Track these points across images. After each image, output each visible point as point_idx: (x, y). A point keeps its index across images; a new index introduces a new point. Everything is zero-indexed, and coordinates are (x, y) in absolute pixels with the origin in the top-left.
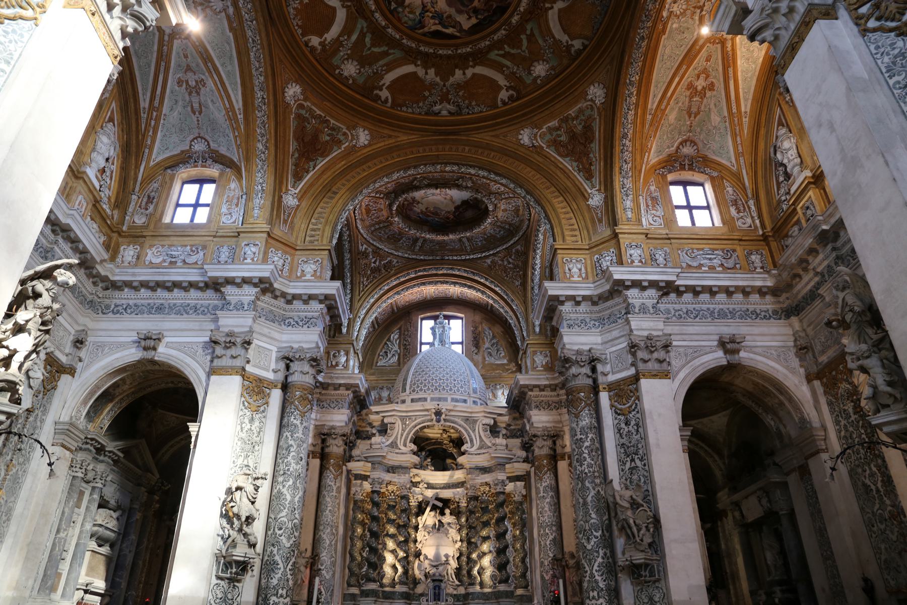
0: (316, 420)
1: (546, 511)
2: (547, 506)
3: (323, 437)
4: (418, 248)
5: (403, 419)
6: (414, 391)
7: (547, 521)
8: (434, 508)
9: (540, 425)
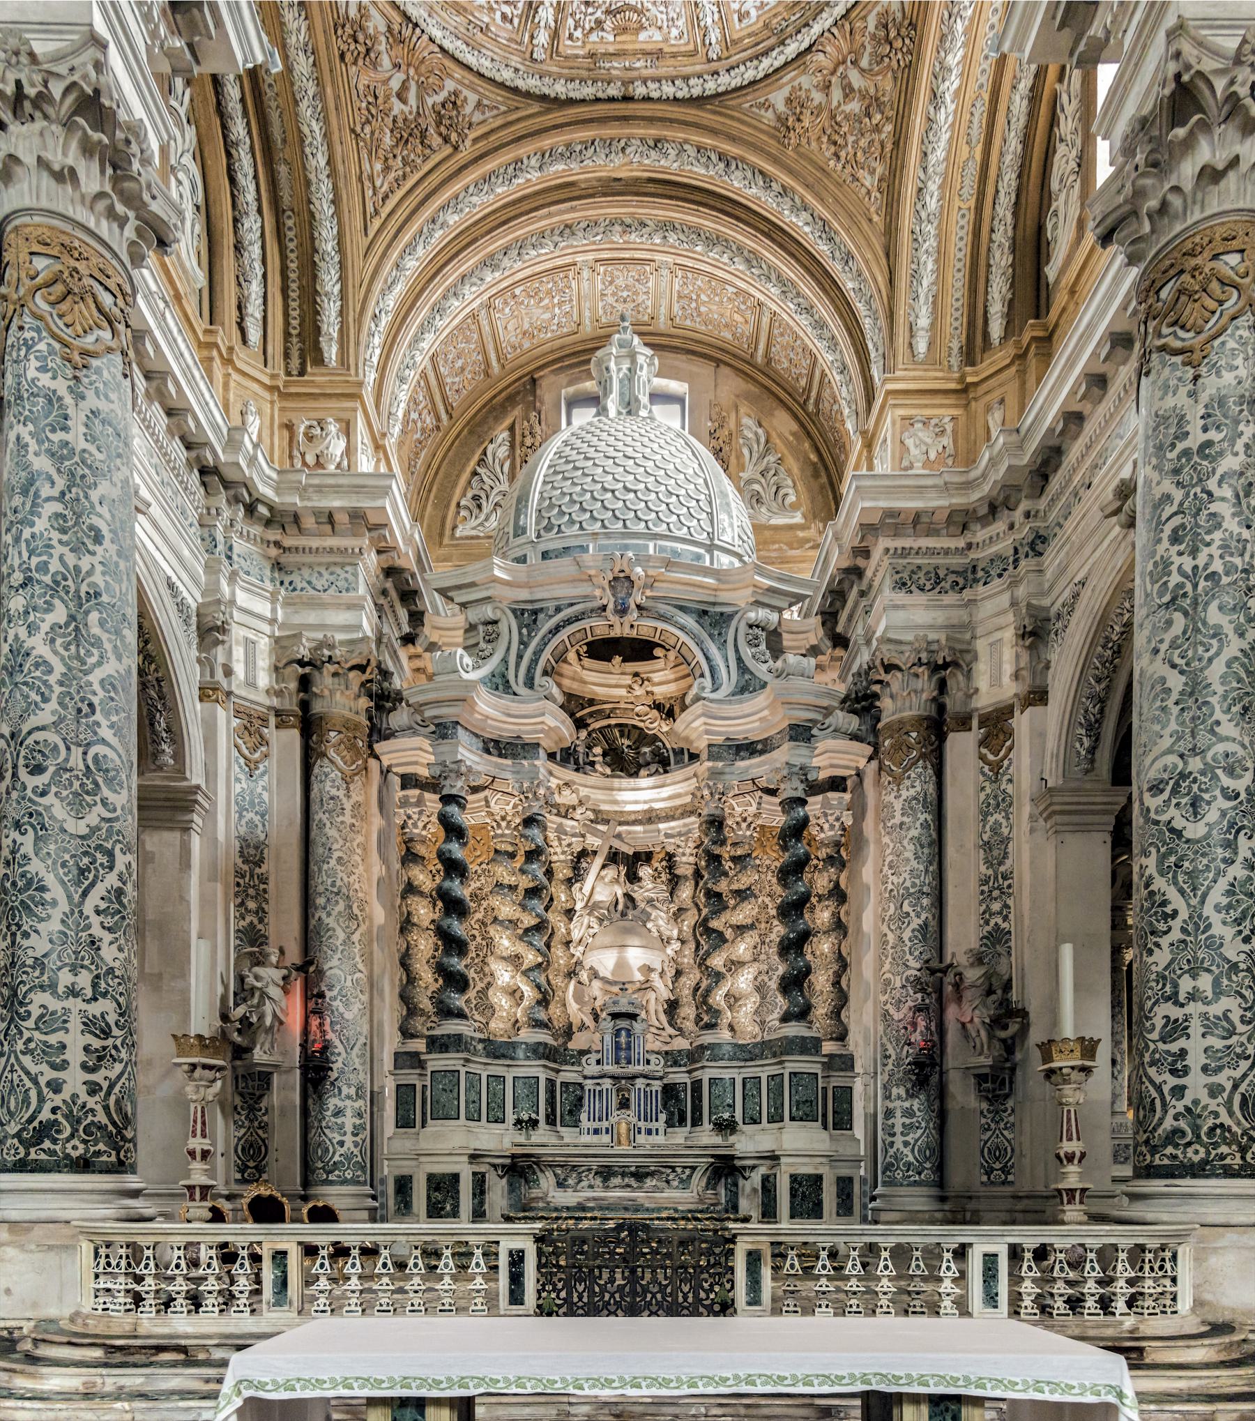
0: (273, 621)
1: (908, 860)
2: (912, 847)
3: (300, 670)
4: (543, 38)
5: (518, 613)
6: (548, 528)
7: (908, 884)
8: (614, 857)
9: (909, 637)
